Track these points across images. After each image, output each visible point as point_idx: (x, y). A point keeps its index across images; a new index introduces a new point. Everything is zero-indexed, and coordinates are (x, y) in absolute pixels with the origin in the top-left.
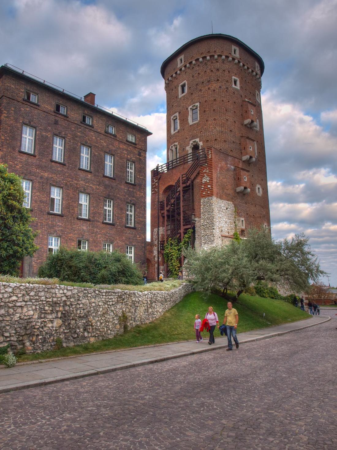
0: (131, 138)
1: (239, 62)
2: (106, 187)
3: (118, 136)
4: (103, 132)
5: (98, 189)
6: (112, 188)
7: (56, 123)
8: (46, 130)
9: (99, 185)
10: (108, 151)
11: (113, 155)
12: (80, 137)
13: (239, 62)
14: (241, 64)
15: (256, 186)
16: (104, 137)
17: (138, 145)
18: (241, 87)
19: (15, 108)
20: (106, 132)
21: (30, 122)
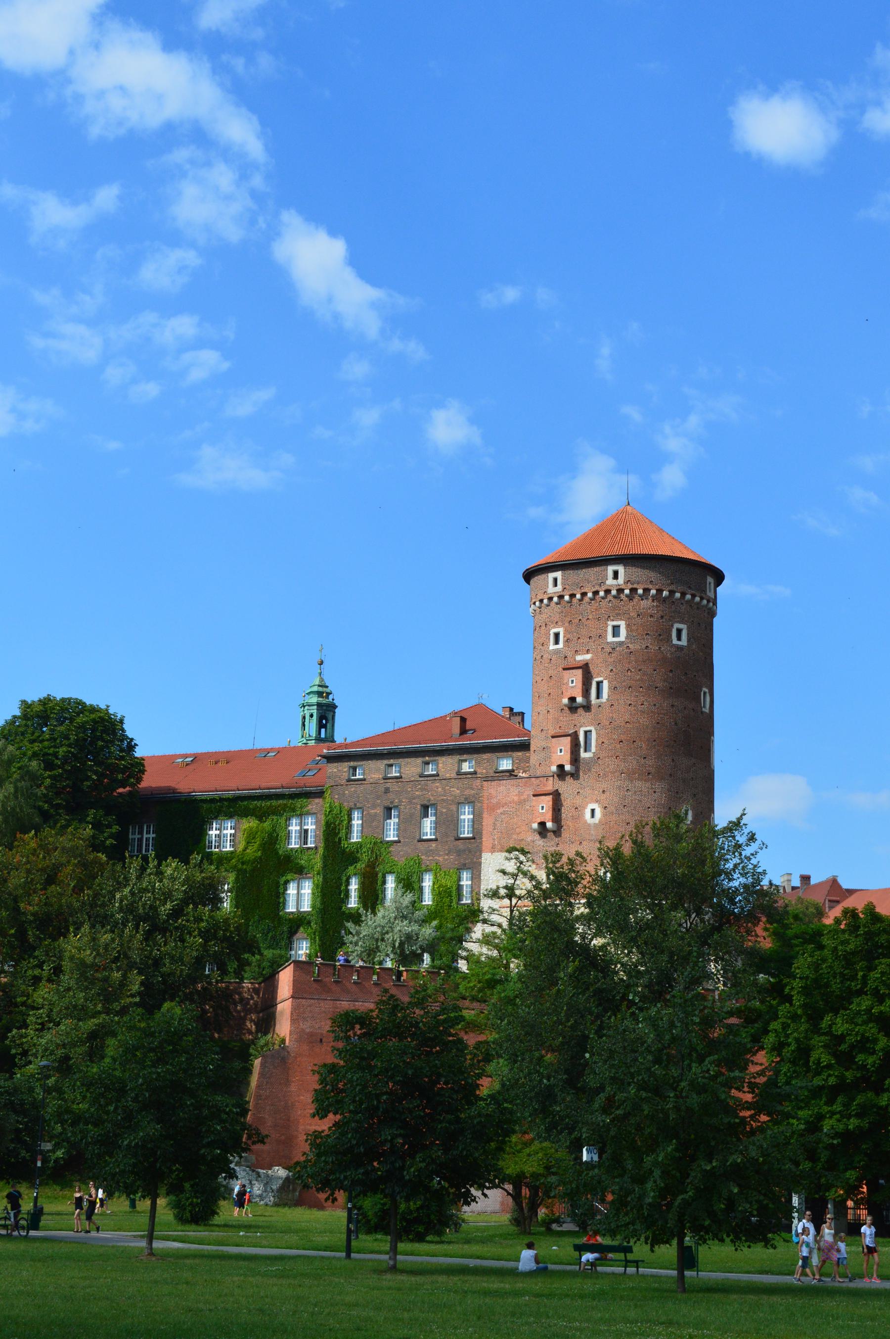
0: (506, 764)
1: (561, 597)
2: (459, 853)
3: (479, 771)
4: (454, 775)
5: (447, 860)
6: (470, 852)
7: (387, 791)
8: (374, 806)
9: (447, 855)
10: (462, 800)
11: (473, 802)
12: (418, 797)
13: (561, 597)
14: (567, 598)
15: (585, 808)
16: (457, 781)
17: (518, 768)
18: (567, 641)
19: (339, 794)
20: (459, 773)
21: (355, 805)
